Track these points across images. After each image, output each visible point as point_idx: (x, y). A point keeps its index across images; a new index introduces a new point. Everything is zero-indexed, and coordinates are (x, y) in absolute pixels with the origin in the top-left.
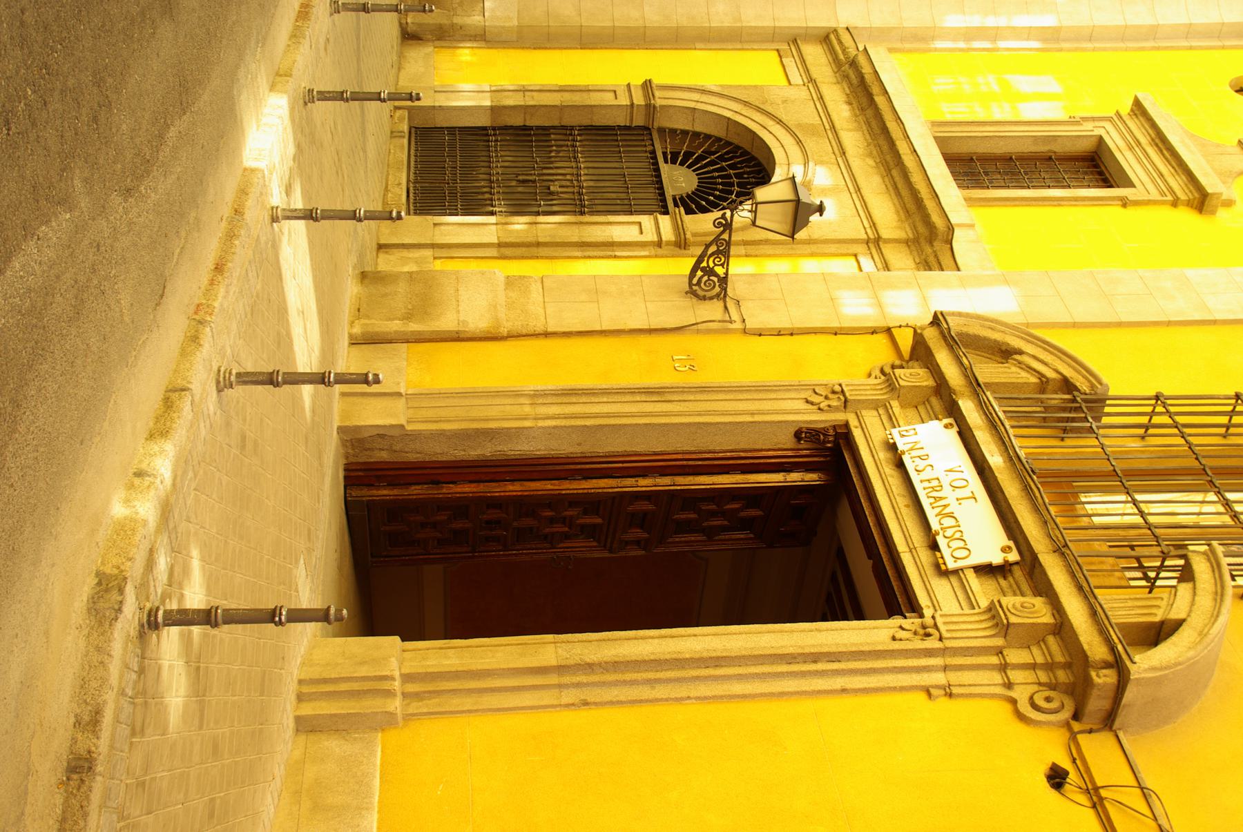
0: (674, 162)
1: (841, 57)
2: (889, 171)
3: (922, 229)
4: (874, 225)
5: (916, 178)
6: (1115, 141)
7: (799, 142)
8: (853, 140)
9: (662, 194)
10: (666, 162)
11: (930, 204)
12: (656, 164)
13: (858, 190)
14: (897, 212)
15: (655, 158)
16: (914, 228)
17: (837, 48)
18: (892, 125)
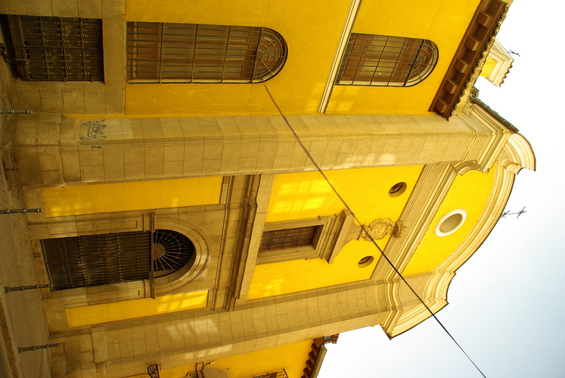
0: (157, 242)
1: (248, 194)
2: (234, 263)
3: (232, 290)
4: (218, 285)
5: (239, 278)
6: (325, 229)
7: (208, 250)
8: (230, 243)
9: (150, 257)
10: (154, 242)
11: (237, 289)
12: (150, 242)
13: (220, 271)
14: (229, 277)
15: (150, 239)
16: (231, 286)
17: (250, 187)
18: (244, 254)
